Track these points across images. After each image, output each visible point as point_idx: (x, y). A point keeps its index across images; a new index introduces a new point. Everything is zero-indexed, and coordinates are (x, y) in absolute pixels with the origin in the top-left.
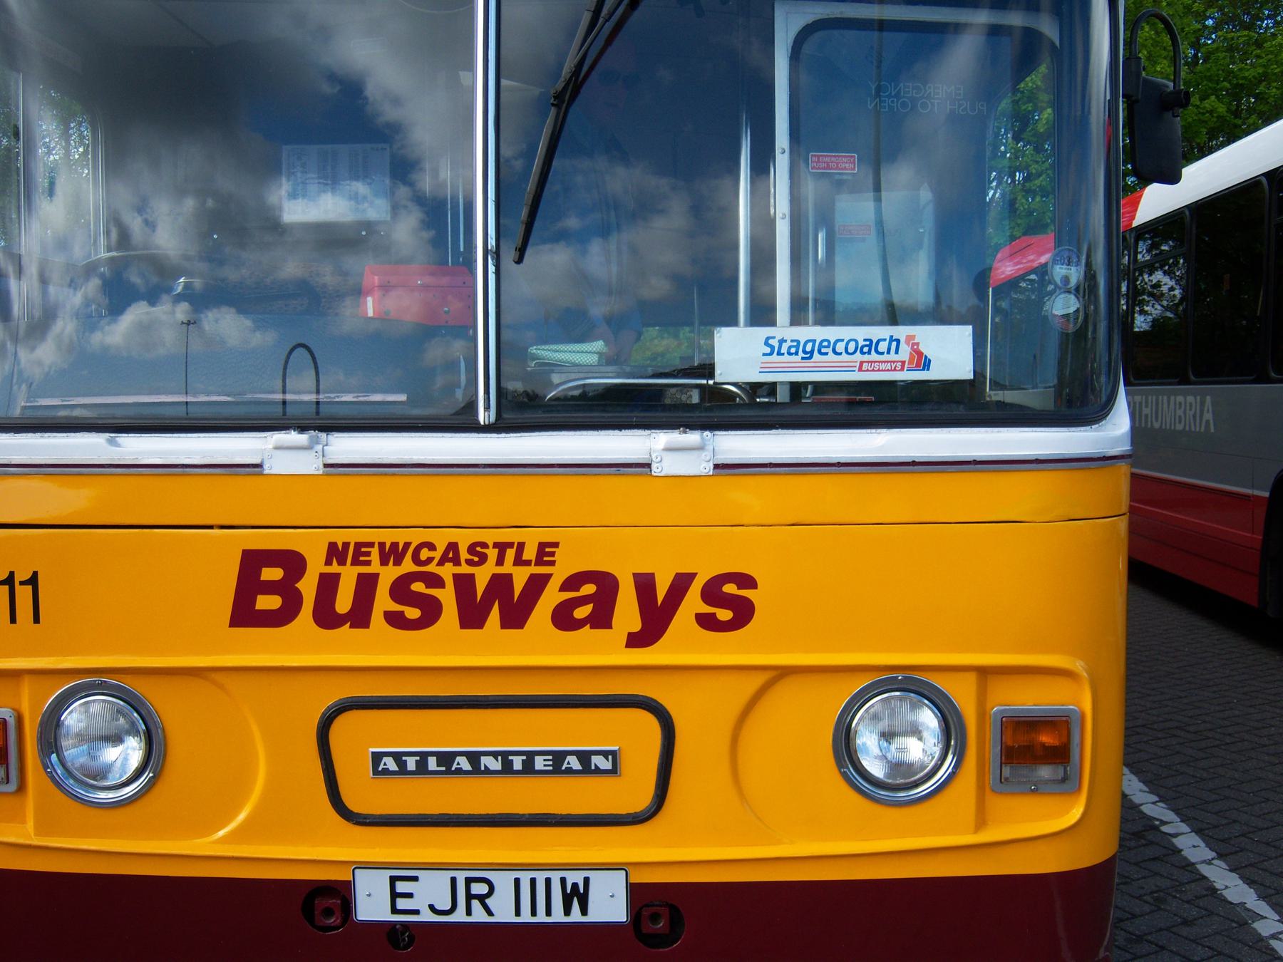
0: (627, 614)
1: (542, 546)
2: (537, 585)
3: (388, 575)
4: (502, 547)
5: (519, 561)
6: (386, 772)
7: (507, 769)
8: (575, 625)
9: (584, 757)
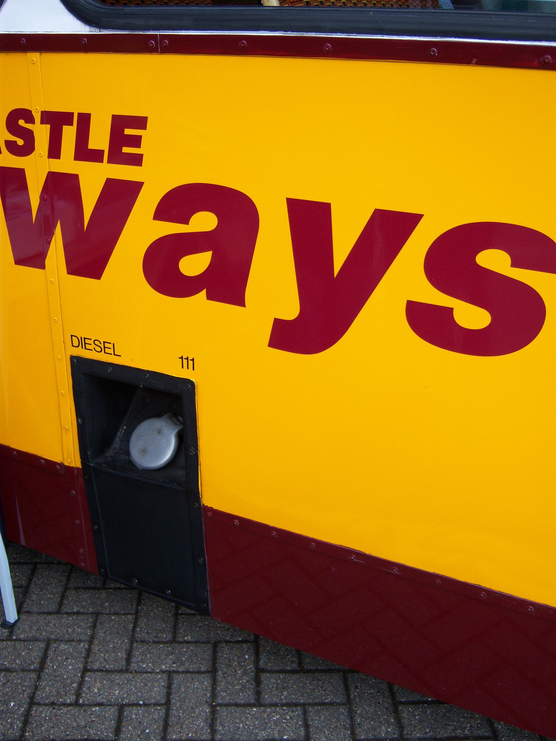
0: (274, 283)
1: (119, 123)
4: (56, 120)
5: (84, 153)
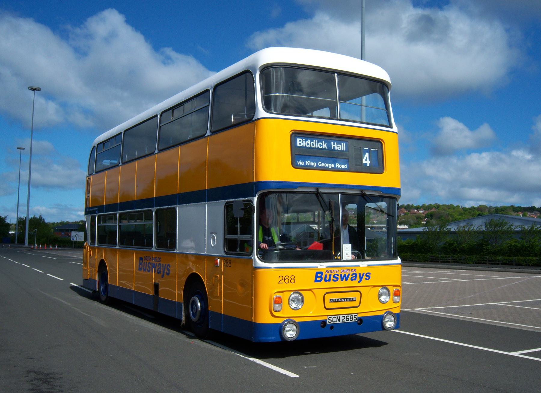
2: (349, 275)
7: (344, 301)
9: (353, 299)
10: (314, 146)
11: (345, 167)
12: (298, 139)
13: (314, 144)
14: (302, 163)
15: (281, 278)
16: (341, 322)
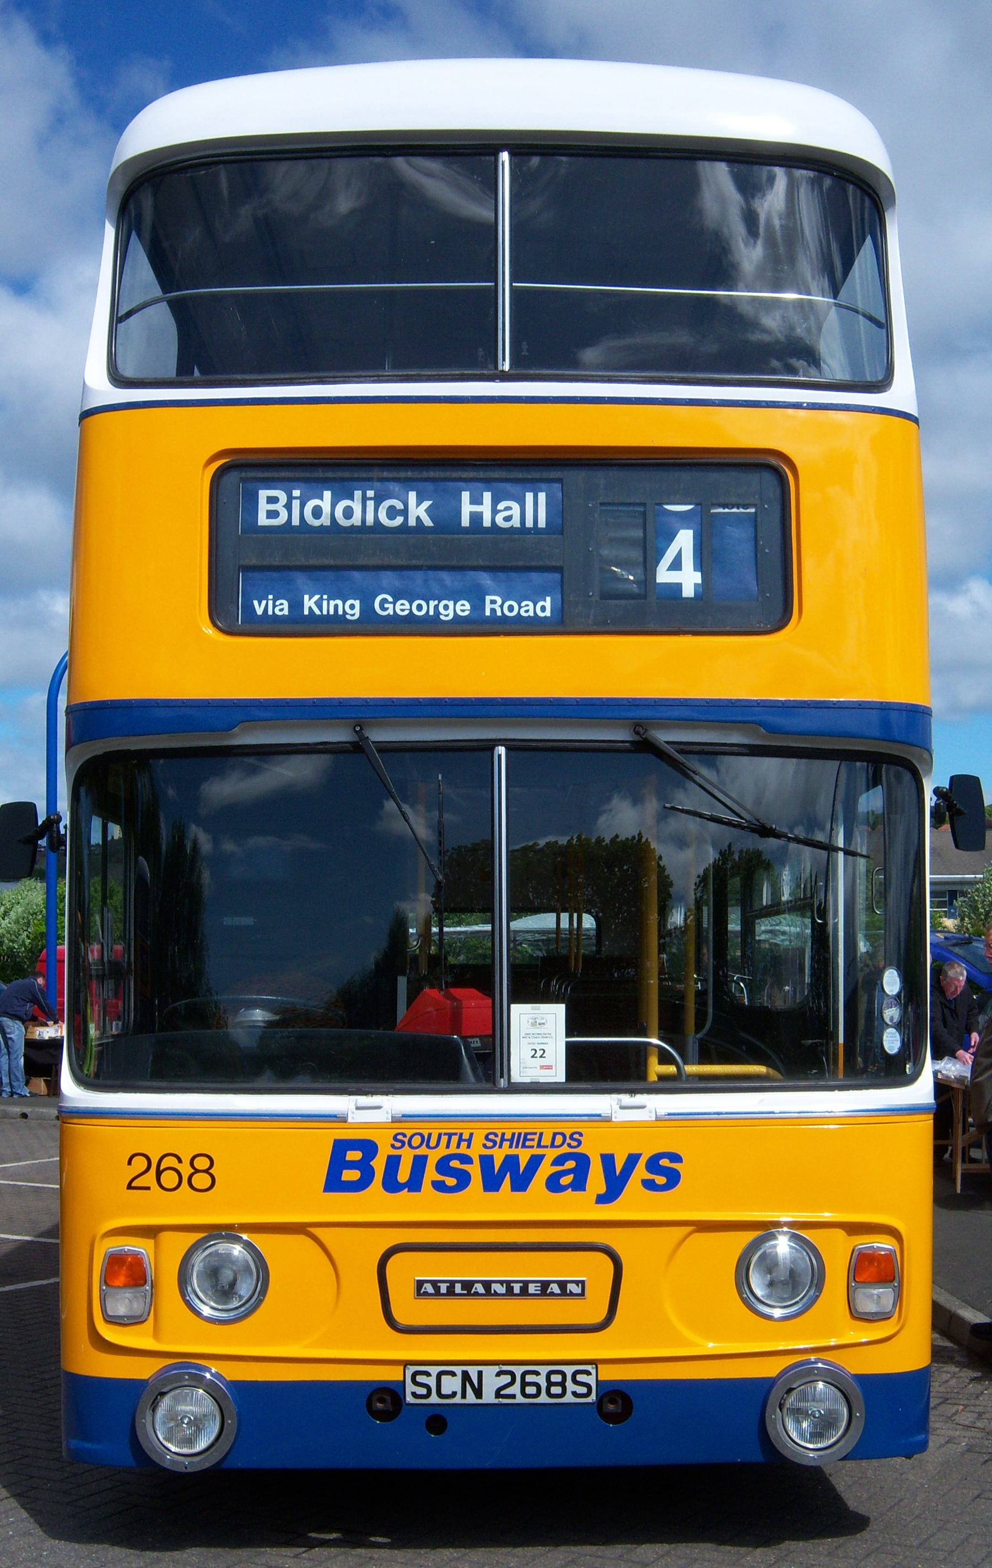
0: (596, 1181)
2: (536, 1161)
3: (434, 1157)
6: (426, 1294)
7: (510, 1292)
8: (562, 1189)
10: (356, 520)
11: (545, 607)
12: (263, 494)
13: (359, 509)
14: (283, 608)
15: (140, 1163)
16: (489, 1397)
